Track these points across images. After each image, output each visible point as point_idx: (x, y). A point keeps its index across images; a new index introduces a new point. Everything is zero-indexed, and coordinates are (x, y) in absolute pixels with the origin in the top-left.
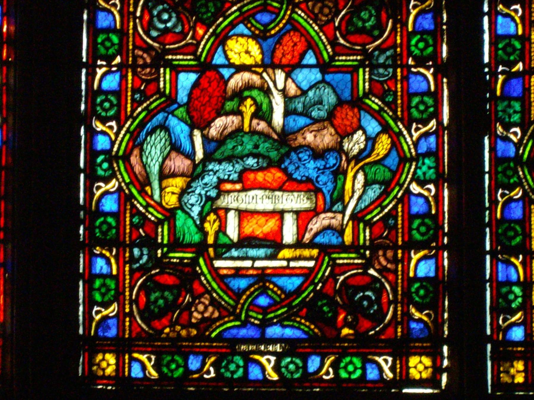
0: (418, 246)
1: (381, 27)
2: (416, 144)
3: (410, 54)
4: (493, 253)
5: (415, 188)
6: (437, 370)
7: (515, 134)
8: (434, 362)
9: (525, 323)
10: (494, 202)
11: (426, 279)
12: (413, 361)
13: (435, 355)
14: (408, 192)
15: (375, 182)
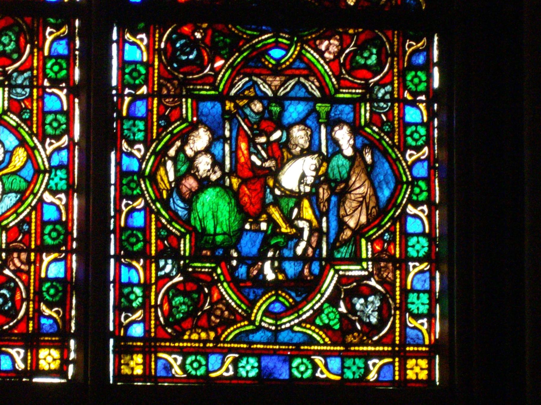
0: (50, 249)
1: (20, 51)
2: (49, 158)
3: (45, 76)
4: (117, 257)
5: (48, 197)
6: (65, 361)
7: (139, 150)
8: (62, 354)
9: (145, 321)
10: (119, 211)
11: (57, 279)
12: (43, 353)
13: (64, 348)
14: (41, 201)
15: (11, 191)
